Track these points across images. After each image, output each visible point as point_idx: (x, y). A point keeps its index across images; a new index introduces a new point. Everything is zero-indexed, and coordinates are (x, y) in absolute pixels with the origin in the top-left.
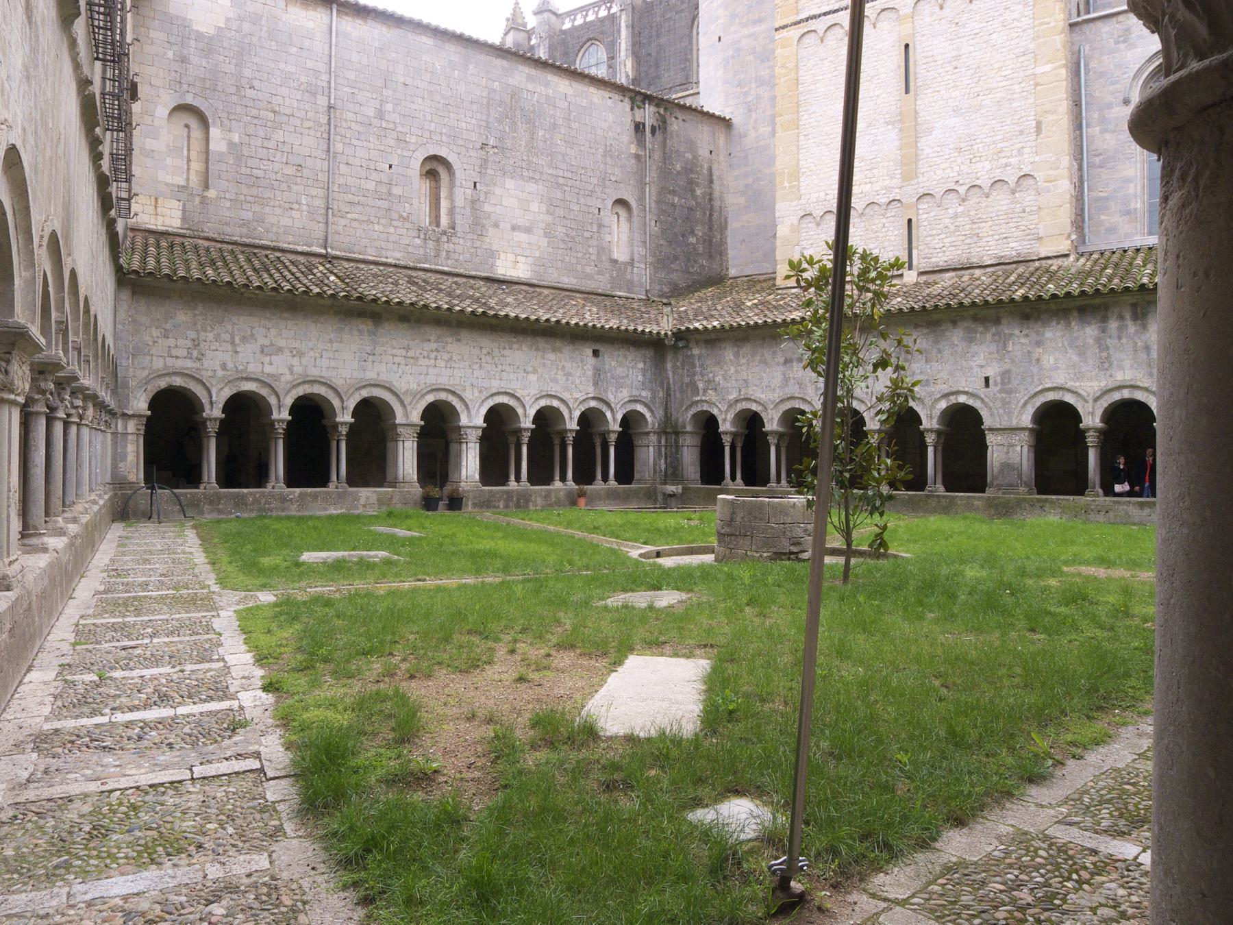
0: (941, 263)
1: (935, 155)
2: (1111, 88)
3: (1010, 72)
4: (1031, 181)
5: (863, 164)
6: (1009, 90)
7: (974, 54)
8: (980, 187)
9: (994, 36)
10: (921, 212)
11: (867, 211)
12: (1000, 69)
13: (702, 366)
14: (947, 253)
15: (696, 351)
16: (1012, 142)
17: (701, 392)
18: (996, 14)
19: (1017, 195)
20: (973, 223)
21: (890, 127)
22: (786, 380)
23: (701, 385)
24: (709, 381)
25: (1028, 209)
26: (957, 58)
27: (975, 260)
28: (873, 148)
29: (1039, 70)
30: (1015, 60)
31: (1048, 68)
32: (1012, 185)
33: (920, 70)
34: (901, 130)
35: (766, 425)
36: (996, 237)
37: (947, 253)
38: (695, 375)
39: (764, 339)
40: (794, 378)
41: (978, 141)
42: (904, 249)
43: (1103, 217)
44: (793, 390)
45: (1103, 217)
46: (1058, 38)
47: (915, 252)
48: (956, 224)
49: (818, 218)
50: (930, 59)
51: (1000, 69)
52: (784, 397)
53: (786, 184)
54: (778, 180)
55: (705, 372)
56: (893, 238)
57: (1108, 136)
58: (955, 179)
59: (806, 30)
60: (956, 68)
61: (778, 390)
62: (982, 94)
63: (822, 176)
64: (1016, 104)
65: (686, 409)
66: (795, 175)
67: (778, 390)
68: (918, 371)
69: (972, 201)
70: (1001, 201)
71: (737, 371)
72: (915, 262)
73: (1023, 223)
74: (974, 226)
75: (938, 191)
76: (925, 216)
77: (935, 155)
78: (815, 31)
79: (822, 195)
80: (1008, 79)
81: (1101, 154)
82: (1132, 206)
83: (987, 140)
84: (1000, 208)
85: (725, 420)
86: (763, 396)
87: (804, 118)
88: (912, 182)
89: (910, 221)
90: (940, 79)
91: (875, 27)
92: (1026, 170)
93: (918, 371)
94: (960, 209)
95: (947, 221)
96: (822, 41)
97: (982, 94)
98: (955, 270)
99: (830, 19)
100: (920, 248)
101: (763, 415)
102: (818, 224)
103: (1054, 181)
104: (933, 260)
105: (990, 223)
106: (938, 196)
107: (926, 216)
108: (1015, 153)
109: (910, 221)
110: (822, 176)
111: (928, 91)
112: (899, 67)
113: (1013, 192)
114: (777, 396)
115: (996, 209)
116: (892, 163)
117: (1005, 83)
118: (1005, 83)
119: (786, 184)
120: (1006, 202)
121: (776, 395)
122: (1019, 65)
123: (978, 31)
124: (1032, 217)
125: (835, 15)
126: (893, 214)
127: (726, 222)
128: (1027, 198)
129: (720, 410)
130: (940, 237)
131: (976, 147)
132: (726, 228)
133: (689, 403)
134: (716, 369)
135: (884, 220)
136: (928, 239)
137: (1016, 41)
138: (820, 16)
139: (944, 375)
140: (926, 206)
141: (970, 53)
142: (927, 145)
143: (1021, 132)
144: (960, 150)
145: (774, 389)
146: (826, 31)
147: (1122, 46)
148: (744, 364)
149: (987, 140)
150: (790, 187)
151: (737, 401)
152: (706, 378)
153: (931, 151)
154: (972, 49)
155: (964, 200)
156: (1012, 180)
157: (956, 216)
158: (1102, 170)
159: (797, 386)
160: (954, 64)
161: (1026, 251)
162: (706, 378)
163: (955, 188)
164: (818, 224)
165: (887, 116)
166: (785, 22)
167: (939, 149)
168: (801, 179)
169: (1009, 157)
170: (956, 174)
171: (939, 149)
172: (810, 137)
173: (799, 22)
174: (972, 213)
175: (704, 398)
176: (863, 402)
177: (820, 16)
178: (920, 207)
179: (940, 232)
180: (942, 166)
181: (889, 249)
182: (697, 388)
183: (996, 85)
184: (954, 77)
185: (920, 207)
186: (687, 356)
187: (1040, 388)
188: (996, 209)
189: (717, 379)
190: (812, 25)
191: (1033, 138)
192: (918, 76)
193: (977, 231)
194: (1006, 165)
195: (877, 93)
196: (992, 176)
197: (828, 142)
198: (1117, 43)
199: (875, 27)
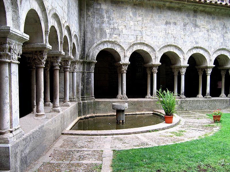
13: (109, 17)
15: (104, 7)
17: (108, 36)
23: (108, 31)
24: (114, 29)
38: (103, 22)
39: (153, 7)
52: (166, 44)
55: (112, 22)
65: (96, 46)
71: (135, 25)
85: (125, 56)
101: (151, 54)
114: (162, 43)
129: (122, 48)
133: (99, 42)
134: (120, 21)
148: (140, 21)
151: (134, 44)
152: (112, 26)
159: (173, 39)
162: (112, 26)
175: (111, 40)
182: (105, 32)
186: (97, 9)
189: (120, 28)
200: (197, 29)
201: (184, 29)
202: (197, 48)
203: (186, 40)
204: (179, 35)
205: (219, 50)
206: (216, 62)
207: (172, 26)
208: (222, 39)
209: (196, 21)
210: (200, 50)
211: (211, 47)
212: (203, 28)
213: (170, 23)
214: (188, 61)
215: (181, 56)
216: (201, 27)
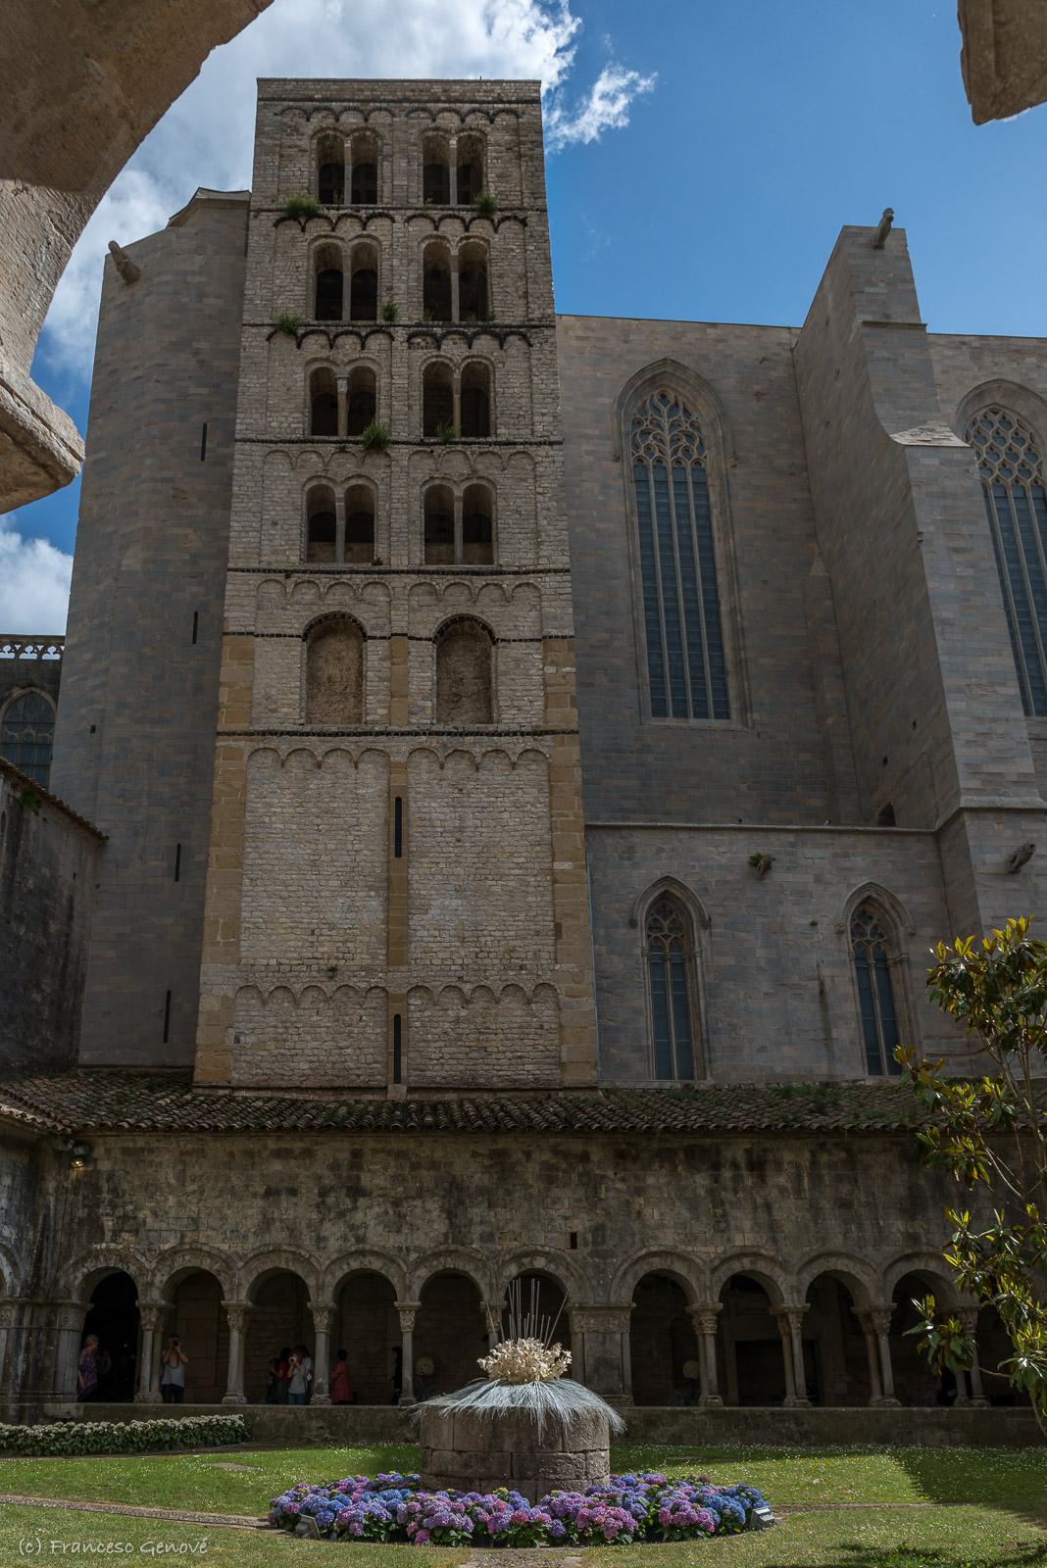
0: (438, 1079)
1: (432, 939)
2: (617, 905)
3: (522, 860)
4: (550, 993)
5: (334, 932)
6: (524, 881)
7: (481, 829)
8: (489, 989)
9: (505, 815)
10: (412, 1008)
11: (338, 995)
12: (512, 854)
14: (447, 1067)
16: (526, 942)
18: (507, 791)
19: (533, 1006)
20: (480, 1033)
21: (373, 893)
22: (266, 1224)
25: (546, 1026)
26: (461, 829)
27: (482, 1081)
28: (349, 915)
29: (559, 866)
30: (529, 848)
31: (567, 866)
32: (529, 994)
33: (414, 832)
34: (388, 899)
35: (227, 1296)
36: (508, 1054)
37: (447, 1067)
40: (281, 1221)
41: (485, 932)
42: (389, 1054)
43: (613, 1051)
44: (278, 1236)
45: (613, 1051)
46: (578, 834)
47: (404, 1059)
48: (458, 1031)
49: (267, 995)
50: (428, 823)
51: (512, 854)
53: (219, 938)
54: (207, 930)
56: (373, 1037)
57: (615, 958)
58: (458, 974)
59: (262, 746)
60: (459, 841)
61: (251, 1239)
62: (490, 877)
63: (274, 937)
64: (530, 899)
66: (234, 927)
67: (251, 1239)
68: (477, 1219)
69: (479, 1005)
70: (513, 1011)
72: (404, 1073)
73: (541, 1042)
74: (481, 1037)
75: (437, 985)
76: (418, 1014)
77: (432, 939)
78: (274, 750)
79: (273, 962)
80: (521, 868)
81: (608, 977)
82: (644, 1042)
83: (497, 933)
84: (513, 1019)
86: (225, 1247)
87: (251, 856)
88: (402, 968)
89: (398, 1017)
90: (439, 849)
91: (356, 767)
92: (547, 977)
93: (477, 1219)
94: (464, 1013)
95: (447, 1025)
96: (283, 765)
97: (490, 877)
98: (455, 1090)
99: (297, 742)
100: (411, 1055)
102: (264, 1003)
103: (578, 997)
104: (428, 1073)
105: (502, 1036)
106: (436, 992)
107: (417, 1011)
108: (530, 955)
109: (398, 1017)
110: (274, 937)
111: (424, 860)
112: (387, 822)
113: (529, 1002)
115: (508, 1019)
116: (374, 939)
117: (517, 872)
118: (517, 872)
119: (219, 938)
120: (519, 1012)
121: (248, 1246)
122: (534, 855)
123: (486, 805)
124: (552, 1036)
125: (305, 738)
126: (374, 1005)
127: (83, 982)
128: (546, 1012)
130: (437, 1044)
131: (483, 939)
132: (82, 990)
135: (361, 1012)
136: (422, 1044)
137: (530, 827)
138: (282, 734)
139: (515, 1226)
140: (419, 1002)
141: (476, 827)
142: (422, 927)
143: (538, 933)
144: (463, 940)
145: (245, 1237)
146: (290, 754)
147: (626, 863)
149: (497, 933)
150: (226, 944)
153: (425, 933)
154: (478, 823)
155: (468, 1002)
156: (528, 988)
157: (457, 1021)
158: (610, 995)
159: (285, 1234)
160: (458, 835)
161: (545, 1077)
163: (458, 984)
164: (264, 1003)
165: (369, 879)
166: (233, 727)
167: (437, 933)
168: (243, 937)
169: (523, 959)
170: (458, 968)
171: (437, 933)
172: (258, 882)
173: (252, 734)
174: (480, 1020)
176: (393, 1261)
177: (282, 734)
178: (412, 1001)
179: (436, 1037)
180: (441, 955)
181: (365, 1051)
183: (507, 872)
184: (456, 851)
185: (412, 1001)
187: (644, 1252)
188: (508, 1019)
190: (273, 742)
191: (551, 942)
192: (412, 839)
193: (485, 1044)
194: (522, 967)
195: (356, 847)
196: (504, 978)
197: (285, 894)
198: (621, 858)
199: (356, 767)
200: (362, 1202)
201: (320, 1206)
202: (362, 1253)
203: (326, 1234)
204: (303, 1223)
205: (436, 1255)
206: (815, 1291)
207: (285, 1201)
208: (447, 1222)
209: (358, 1178)
210: (371, 1258)
211: (407, 1248)
212: (381, 1196)
213: (278, 1193)
214: (895, 1293)
215: (311, 1282)
216: (375, 1194)
